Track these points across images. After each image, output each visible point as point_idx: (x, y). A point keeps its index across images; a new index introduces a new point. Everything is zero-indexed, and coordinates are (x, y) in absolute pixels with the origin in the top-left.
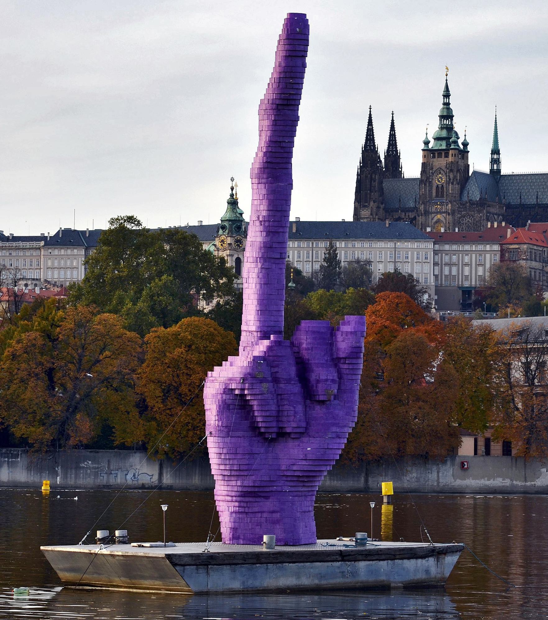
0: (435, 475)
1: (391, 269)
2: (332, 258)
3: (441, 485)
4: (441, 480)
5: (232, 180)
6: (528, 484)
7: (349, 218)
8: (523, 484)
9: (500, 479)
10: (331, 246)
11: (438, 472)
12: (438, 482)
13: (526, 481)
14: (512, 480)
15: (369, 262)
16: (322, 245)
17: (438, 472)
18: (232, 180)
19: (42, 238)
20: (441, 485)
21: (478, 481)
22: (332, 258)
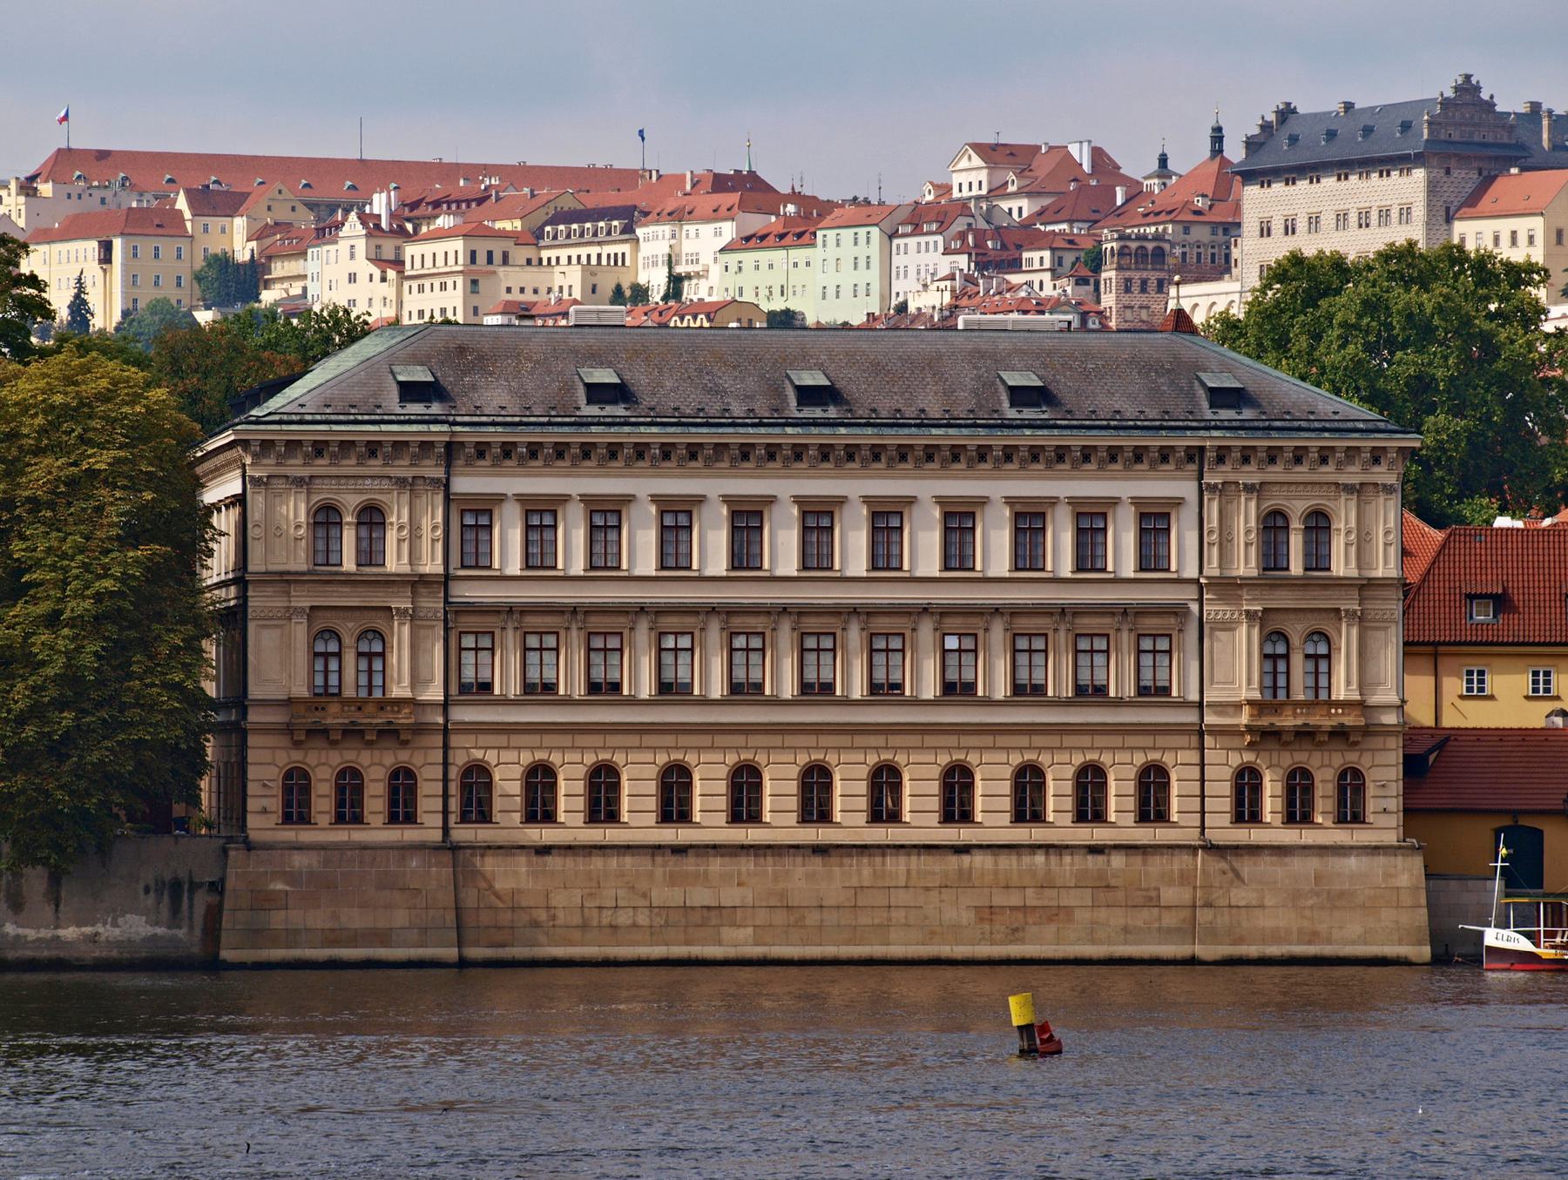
8: (45, 933)
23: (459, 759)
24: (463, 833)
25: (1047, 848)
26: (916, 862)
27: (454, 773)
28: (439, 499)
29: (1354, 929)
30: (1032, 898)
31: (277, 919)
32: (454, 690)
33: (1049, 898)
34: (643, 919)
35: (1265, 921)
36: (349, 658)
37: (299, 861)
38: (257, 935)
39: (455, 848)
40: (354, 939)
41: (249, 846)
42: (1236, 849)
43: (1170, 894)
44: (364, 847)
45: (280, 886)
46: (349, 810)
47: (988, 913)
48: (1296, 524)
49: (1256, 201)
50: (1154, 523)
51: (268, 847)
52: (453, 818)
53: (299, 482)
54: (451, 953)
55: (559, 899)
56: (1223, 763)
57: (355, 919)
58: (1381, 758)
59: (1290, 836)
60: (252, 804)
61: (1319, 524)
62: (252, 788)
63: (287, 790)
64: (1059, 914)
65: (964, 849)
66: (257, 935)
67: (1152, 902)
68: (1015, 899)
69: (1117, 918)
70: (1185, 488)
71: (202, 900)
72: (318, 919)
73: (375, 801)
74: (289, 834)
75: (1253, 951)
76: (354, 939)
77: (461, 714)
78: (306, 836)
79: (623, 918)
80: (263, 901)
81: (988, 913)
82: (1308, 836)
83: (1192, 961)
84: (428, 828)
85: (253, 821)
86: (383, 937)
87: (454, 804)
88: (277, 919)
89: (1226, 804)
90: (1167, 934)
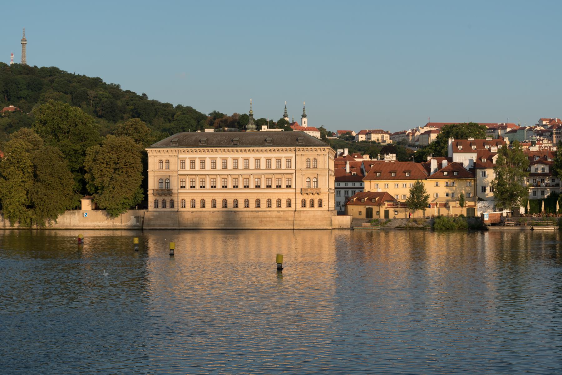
9: (107, 222)
11: (70, 219)
12: (70, 224)
17: (70, 219)
24: (180, 209)
26: (251, 214)
27: (179, 201)
28: (177, 159)
30: (268, 219)
31: (152, 223)
32: (179, 187)
33: (271, 219)
36: (311, 182)
40: (163, 225)
43: (290, 219)
44: (165, 211)
46: (164, 207)
48: (164, 162)
50: (289, 160)
53: (156, 156)
54: (177, 228)
56: (300, 198)
57: (163, 222)
58: (325, 197)
61: (315, 160)
63: (155, 203)
69: (282, 222)
70: (292, 155)
73: (168, 205)
77: (180, 191)
82: (313, 209)
86: (167, 225)
90: (290, 225)
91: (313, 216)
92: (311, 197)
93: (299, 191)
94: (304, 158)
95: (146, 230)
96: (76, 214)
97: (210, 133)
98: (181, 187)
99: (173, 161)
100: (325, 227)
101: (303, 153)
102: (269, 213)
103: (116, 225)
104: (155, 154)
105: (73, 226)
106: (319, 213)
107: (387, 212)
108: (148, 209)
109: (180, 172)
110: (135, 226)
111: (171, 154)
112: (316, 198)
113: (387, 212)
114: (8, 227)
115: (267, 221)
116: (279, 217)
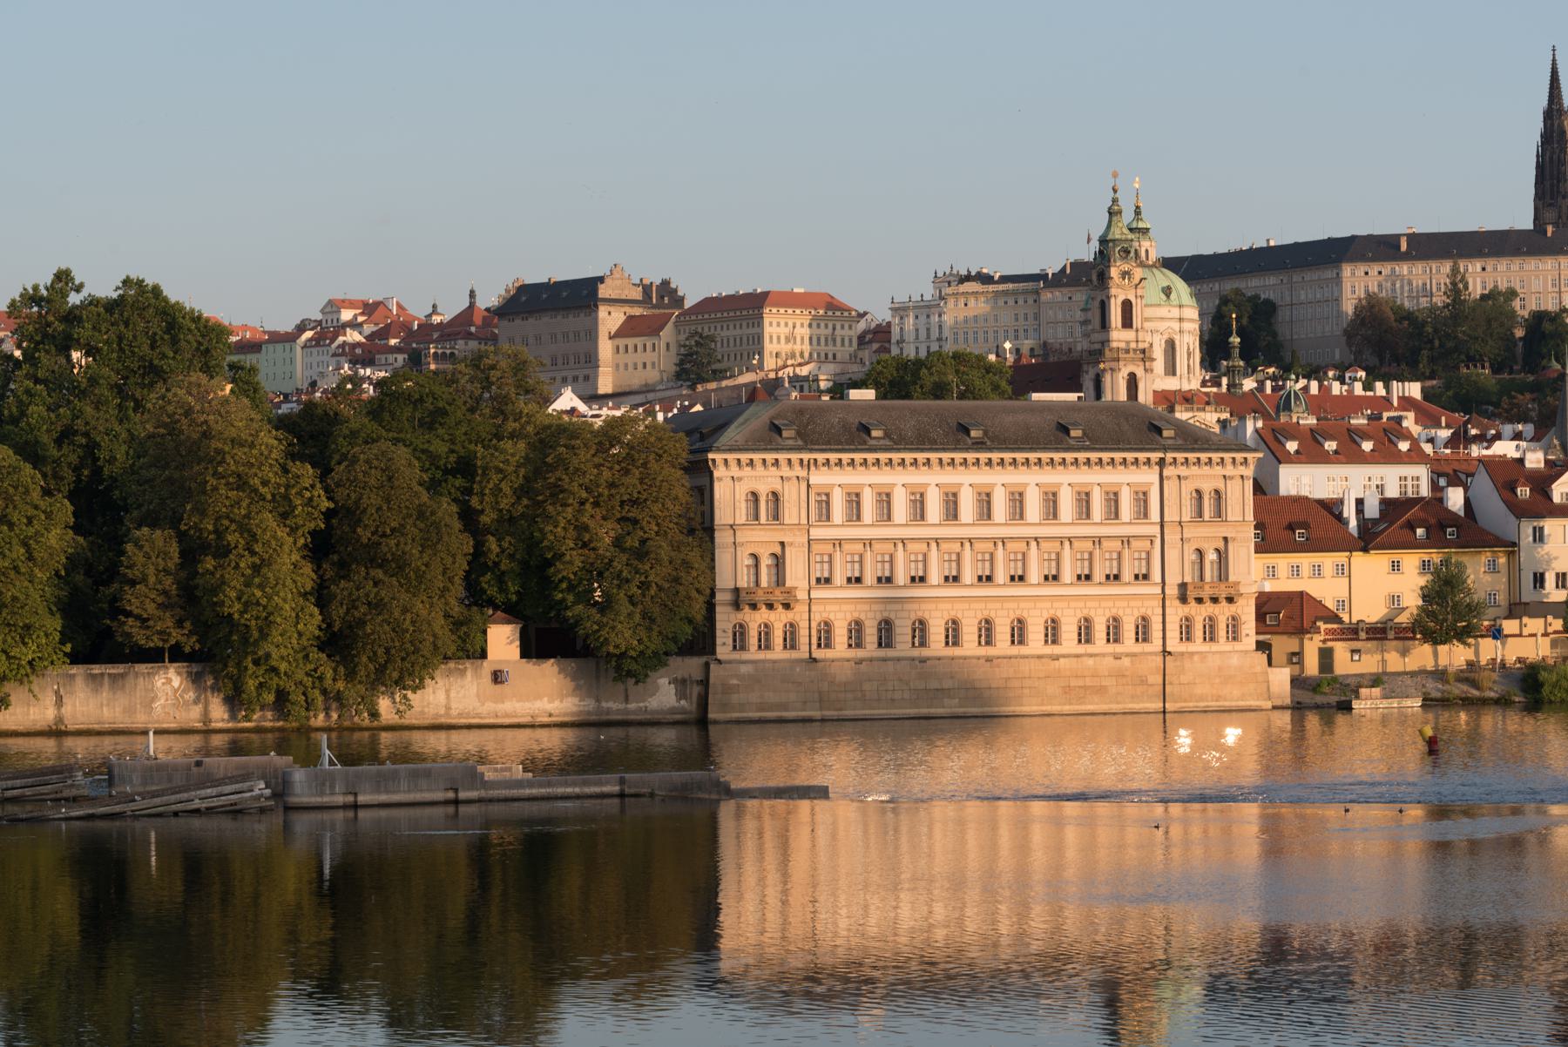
0: (441, 697)
1: (1551, 306)
2: (1456, 288)
3: (454, 713)
4: (454, 705)
5: (1115, 175)
6: (632, 706)
7: (1528, 224)
8: (622, 706)
10: (1455, 270)
11: (448, 691)
12: (448, 708)
13: (627, 700)
14: (598, 701)
15: (1512, 293)
16: (1446, 267)
17: (448, 691)
18: (1115, 175)
19: (1042, 277)
20: (454, 713)
21: (528, 705)
22: (1456, 288)
23: (817, 618)
24: (817, 654)
25: (1091, 655)
26: (1034, 664)
27: (814, 625)
29: (1236, 693)
31: (735, 698)
32: (813, 582)
34: (906, 696)
35: (1198, 690)
37: (744, 669)
38: (725, 707)
39: (815, 660)
40: (771, 708)
41: (720, 662)
42: (1182, 654)
45: (735, 682)
47: (1067, 690)
49: (502, 329)
51: (730, 662)
52: (814, 646)
53: (740, 479)
54: (817, 714)
55: (867, 686)
57: (771, 697)
59: (1206, 647)
60: (719, 641)
62: (719, 633)
64: (1101, 690)
65: (1056, 658)
66: (725, 707)
67: (1143, 681)
68: (1081, 683)
71: (696, 690)
72: (754, 697)
74: (736, 656)
75: (1191, 705)
76: (771, 708)
78: (745, 656)
79: (897, 695)
80: (728, 689)
81: (1067, 690)
82: (1214, 647)
83: (810, 720)
84: (802, 653)
85: (719, 649)
86: (784, 707)
87: (814, 641)
88: (735, 698)
89: (875, 639)
91: (1220, 669)
92: (1208, 609)
93: (1172, 591)
94: (1188, 488)
95: (716, 722)
96: (469, 673)
97: (863, 406)
98: (818, 580)
99: (792, 497)
100: (1253, 703)
101: (1183, 471)
102: (1090, 662)
103: (608, 711)
104: (734, 471)
105: (460, 715)
106: (1235, 661)
107: (1326, 656)
108: (714, 652)
109: (816, 533)
110: (673, 711)
111: (785, 471)
112: (1223, 612)
113: (1326, 656)
114: (220, 725)
115: (1085, 688)
116: (1120, 675)
